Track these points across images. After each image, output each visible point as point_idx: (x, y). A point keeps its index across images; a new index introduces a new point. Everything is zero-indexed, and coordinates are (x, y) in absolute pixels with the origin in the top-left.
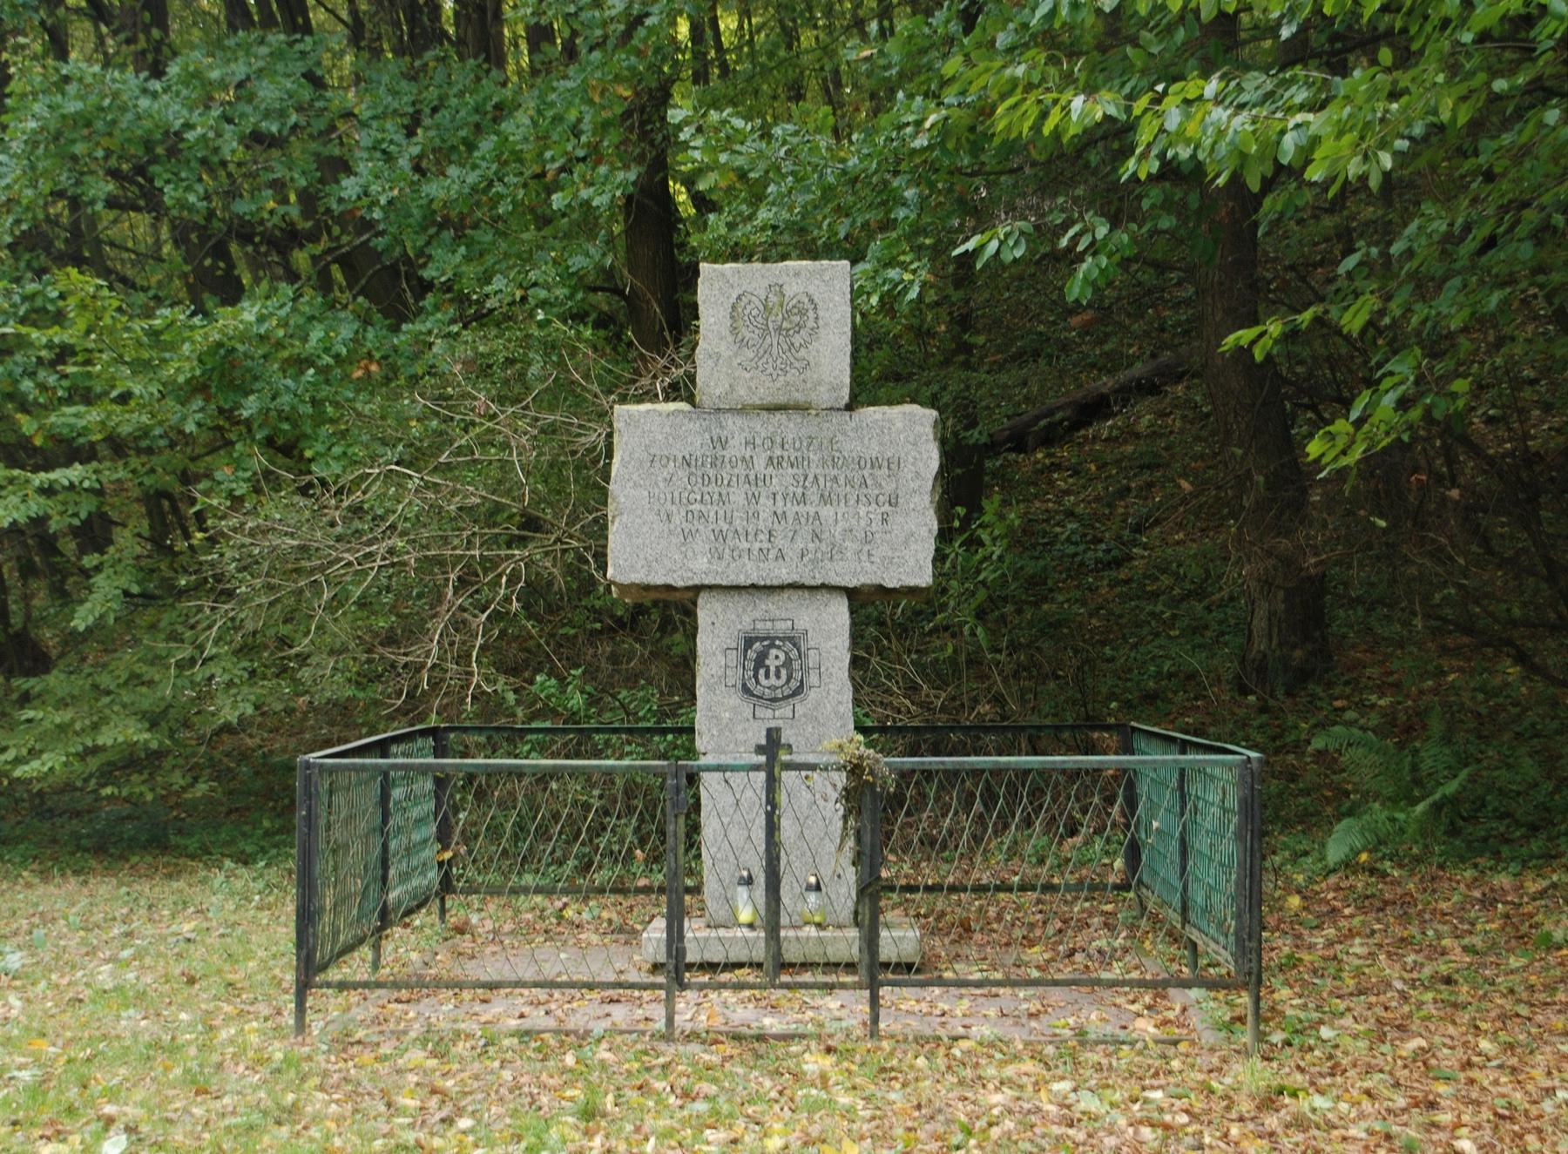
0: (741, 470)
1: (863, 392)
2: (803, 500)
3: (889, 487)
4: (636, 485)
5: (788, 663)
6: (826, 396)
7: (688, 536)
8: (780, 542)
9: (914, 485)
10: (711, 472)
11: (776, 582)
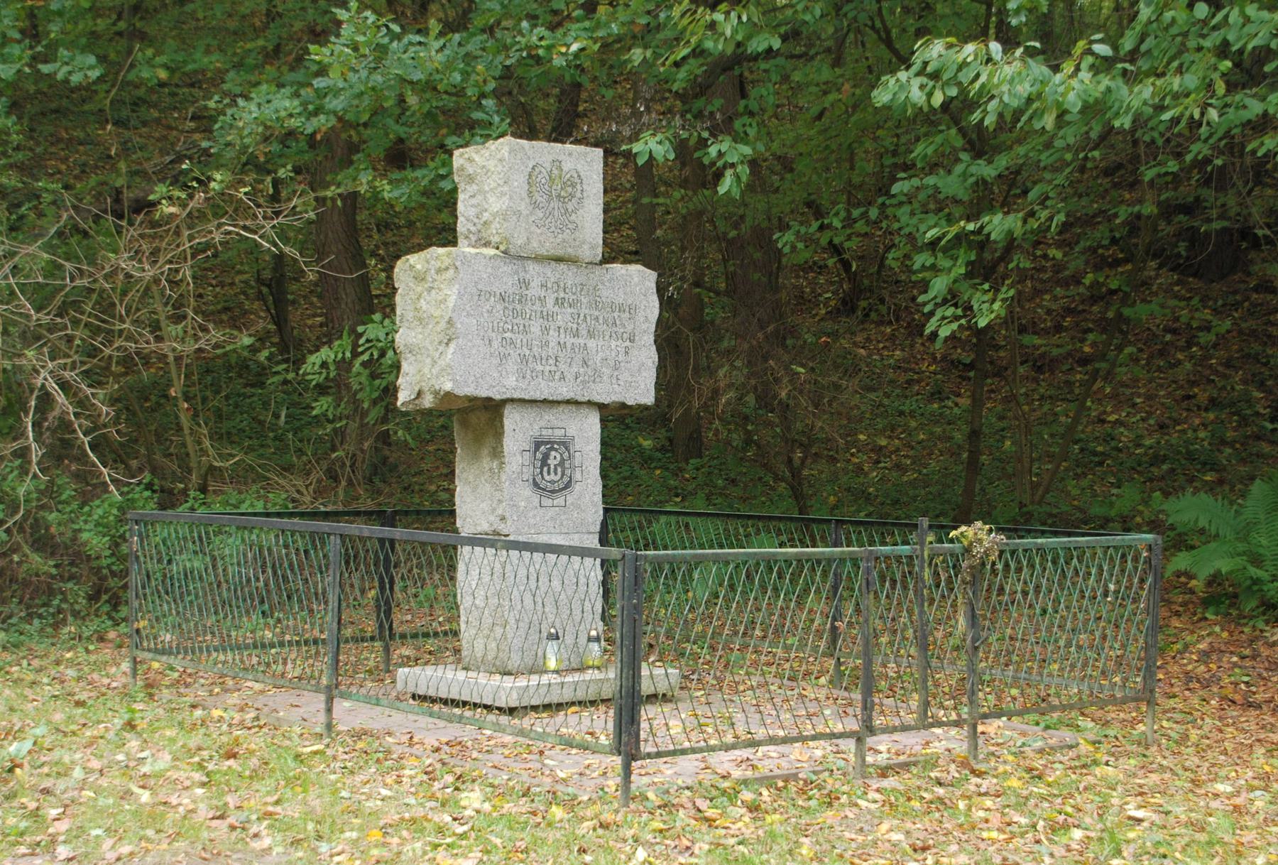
0: (537, 307)
1: (613, 254)
2: (576, 334)
3: (630, 328)
4: (468, 315)
5: (563, 460)
6: (588, 253)
7: (504, 357)
8: (562, 367)
9: (644, 327)
10: (519, 307)
11: (560, 398)
